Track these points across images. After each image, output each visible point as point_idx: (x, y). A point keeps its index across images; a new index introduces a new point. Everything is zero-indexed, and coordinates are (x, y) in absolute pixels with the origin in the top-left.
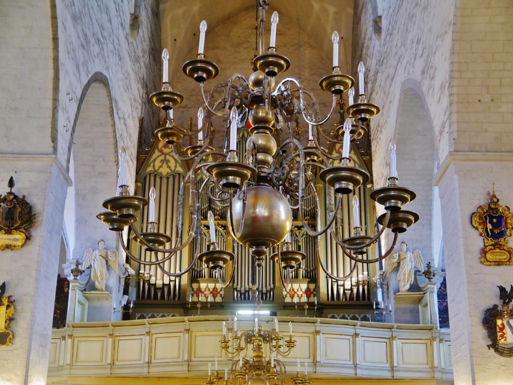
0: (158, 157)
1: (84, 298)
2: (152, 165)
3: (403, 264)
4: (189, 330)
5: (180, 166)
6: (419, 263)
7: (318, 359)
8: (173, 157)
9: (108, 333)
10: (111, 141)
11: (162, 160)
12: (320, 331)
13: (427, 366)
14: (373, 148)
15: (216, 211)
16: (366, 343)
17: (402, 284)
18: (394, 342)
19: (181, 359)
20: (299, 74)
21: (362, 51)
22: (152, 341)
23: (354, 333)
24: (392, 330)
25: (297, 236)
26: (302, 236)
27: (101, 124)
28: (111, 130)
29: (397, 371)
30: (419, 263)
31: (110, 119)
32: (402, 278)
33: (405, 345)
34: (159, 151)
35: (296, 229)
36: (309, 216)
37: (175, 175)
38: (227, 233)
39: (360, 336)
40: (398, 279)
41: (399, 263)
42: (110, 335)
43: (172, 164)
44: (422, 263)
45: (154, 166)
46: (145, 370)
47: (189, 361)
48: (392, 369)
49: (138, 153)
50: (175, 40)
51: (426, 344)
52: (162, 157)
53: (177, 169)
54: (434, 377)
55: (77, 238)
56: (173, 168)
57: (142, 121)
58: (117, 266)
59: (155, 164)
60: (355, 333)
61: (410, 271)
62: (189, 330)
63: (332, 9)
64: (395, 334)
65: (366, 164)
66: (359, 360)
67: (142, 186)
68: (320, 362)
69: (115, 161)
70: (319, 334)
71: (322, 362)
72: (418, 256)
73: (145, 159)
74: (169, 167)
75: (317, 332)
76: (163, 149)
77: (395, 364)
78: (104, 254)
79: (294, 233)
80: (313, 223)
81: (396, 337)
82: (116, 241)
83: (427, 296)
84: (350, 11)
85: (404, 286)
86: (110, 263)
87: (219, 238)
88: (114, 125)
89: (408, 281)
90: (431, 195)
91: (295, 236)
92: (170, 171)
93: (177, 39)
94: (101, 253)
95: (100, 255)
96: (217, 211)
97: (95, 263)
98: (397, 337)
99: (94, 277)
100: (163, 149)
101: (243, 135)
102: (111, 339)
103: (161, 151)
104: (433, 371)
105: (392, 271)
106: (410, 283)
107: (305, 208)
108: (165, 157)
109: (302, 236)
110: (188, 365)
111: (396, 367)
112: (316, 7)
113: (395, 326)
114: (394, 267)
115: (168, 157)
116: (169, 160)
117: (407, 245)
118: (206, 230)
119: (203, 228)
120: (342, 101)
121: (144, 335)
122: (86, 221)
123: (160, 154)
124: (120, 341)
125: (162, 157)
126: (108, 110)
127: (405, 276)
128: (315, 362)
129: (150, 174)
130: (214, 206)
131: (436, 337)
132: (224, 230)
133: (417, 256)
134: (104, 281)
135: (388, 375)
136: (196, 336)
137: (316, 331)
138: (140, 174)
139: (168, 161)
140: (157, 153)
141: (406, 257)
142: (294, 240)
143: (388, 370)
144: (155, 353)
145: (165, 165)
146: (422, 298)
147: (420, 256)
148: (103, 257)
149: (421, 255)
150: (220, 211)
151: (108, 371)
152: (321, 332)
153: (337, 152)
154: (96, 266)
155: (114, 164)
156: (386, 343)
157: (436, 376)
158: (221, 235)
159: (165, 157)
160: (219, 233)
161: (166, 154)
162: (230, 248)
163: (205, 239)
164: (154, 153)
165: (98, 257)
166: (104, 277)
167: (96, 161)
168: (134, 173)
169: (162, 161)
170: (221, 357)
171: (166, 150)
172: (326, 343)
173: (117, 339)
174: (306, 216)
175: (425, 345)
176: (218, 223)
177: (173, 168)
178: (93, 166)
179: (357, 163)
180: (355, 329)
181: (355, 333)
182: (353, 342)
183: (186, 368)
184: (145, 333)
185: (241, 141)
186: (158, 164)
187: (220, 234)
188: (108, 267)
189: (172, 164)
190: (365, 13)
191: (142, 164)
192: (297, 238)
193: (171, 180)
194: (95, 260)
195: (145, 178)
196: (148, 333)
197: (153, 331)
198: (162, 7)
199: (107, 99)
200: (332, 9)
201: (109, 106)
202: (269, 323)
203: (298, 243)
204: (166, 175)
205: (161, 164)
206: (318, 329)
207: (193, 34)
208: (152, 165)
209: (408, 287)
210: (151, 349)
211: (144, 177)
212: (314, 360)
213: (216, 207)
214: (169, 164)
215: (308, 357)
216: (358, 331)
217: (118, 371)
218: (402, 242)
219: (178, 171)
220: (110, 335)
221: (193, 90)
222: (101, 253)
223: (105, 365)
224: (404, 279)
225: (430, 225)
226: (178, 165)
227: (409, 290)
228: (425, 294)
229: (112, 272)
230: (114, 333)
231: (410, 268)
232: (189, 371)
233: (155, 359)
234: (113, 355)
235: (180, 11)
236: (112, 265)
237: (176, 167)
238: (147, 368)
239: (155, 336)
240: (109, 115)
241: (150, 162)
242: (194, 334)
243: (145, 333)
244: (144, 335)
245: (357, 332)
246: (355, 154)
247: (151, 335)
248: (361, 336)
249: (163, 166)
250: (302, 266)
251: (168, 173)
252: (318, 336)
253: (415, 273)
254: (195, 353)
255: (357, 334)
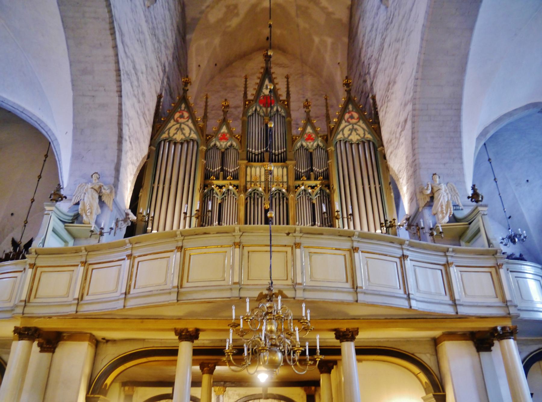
0: (173, 125)
1: (66, 232)
2: (167, 132)
3: (439, 195)
4: (182, 247)
5: (195, 133)
6: (455, 197)
7: (359, 284)
8: (188, 126)
9: (80, 261)
10: (112, 66)
11: (177, 128)
12: (358, 248)
13: (496, 300)
14: (381, 115)
15: (228, 173)
16: (418, 269)
17: (440, 216)
18: (451, 269)
19: (169, 286)
20: (303, 95)
21: (360, 56)
22: (133, 266)
23: (401, 254)
24: (448, 254)
25: (310, 195)
26: (316, 195)
27: (101, 44)
28: (111, 52)
29: (460, 305)
30: (455, 197)
31: (110, 38)
32: (440, 210)
33: (464, 274)
34: (174, 121)
35: (310, 188)
36: (322, 176)
37: (189, 140)
38: (239, 192)
39: (408, 259)
40: (435, 212)
41: (432, 198)
42: (82, 263)
43: (187, 131)
44: (458, 198)
45: (169, 134)
46: (120, 304)
47: (179, 287)
48: (454, 304)
49: (154, 122)
50: (199, 66)
51: (491, 272)
52: (178, 126)
53: (191, 136)
54: (509, 314)
55: (71, 175)
56: (187, 135)
57: (160, 97)
58: (112, 200)
59: (170, 131)
60: (403, 255)
61: (448, 202)
62: (182, 247)
63: (329, 41)
64: (450, 260)
65: (376, 131)
66: (412, 290)
67: (156, 149)
68: (361, 288)
69: (117, 91)
70: (357, 252)
71: (364, 288)
72: (453, 190)
73: (160, 127)
74: (184, 134)
75: (355, 249)
76: (178, 119)
77: (457, 297)
78: (97, 187)
79: (307, 192)
80: (326, 182)
81: (452, 263)
82: (115, 177)
83: (479, 221)
84: (346, 40)
85: (443, 218)
86: (104, 199)
87: (231, 197)
88: (115, 47)
89: (446, 214)
90: (460, 126)
91: (308, 195)
92: (184, 137)
93: (201, 65)
94: (94, 185)
95: (92, 188)
96: (230, 173)
97: (86, 195)
98: (454, 264)
99: (82, 211)
100: (178, 119)
101: (256, 110)
102: (83, 268)
103: (177, 122)
104: (507, 306)
105: (425, 206)
106: (449, 216)
107: (318, 170)
108: (180, 126)
109: (316, 195)
110: (178, 293)
111: (459, 300)
112: (316, 39)
113: (451, 250)
114: (426, 202)
115: (183, 126)
116: (183, 129)
117: (439, 177)
118: (218, 189)
119: (215, 188)
120: (347, 81)
121: (124, 259)
122: (83, 157)
123: (175, 123)
124: (94, 271)
125: (178, 126)
126: (107, 26)
127: (442, 208)
128: (355, 288)
129: (165, 140)
130: (227, 169)
131: (502, 264)
132: (236, 189)
133: (451, 190)
134: (94, 217)
135: (450, 311)
136: (190, 256)
137: (353, 247)
138: (155, 140)
139: (182, 129)
140: (172, 122)
141: (440, 188)
142: (308, 199)
143: (449, 305)
144: (135, 281)
145: (179, 132)
146: (468, 228)
147: (454, 190)
148: (95, 190)
149: (455, 189)
150: (233, 173)
151: (72, 309)
152: (360, 249)
153: (346, 122)
154: (86, 199)
155: (116, 94)
156: (441, 270)
157: (511, 312)
158: (234, 194)
159: (180, 126)
160: (231, 193)
161: (181, 124)
162: (242, 205)
163: (217, 198)
164: (170, 122)
165: (90, 190)
166: (94, 212)
167: (96, 91)
168: (149, 138)
169: (177, 129)
170: (224, 280)
171: (182, 120)
172: (367, 264)
173: (91, 267)
174: (319, 176)
175: (489, 274)
176: (230, 183)
177: (187, 135)
178: (93, 96)
179: (366, 131)
180: (402, 249)
181: (403, 255)
182: (402, 267)
183: (174, 297)
184: (125, 257)
185: (254, 115)
186: (172, 131)
187: (232, 193)
188: (101, 203)
189: (187, 131)
190: (363, 20)
191: (157, 131)
192: (310, 197)
193: (185, 145)
194: (87, 193)
195: (160, 143)
196: (130, 256)
197: (136, 253)
198: (188, 37)
199: (106, 10)
200: (329, 41)
201: (108, 20)
202: (290, 235)
203: (311, 202)
204: (180, 141)
205: (175, 131)
206: (356, 245)
207: (215, 64)
208: (167, 132)
209: (447, 219)
210: (131, 276)
211: (158, 142)
212: (353, 285)
213: (229, 170)
214: (184, 132)
215: (345, 280)
216: (406, 253)
217: (85, 309)
218: (434, 174)
219: (192, 137)
220: (82, 263)
221: (214, 106)
222: (94, 185)
223: (71, 301)
224: (442, 212)
225: (461, 158)
226: (192, 132)
227: (449, 222)
228: (470, 224)
229: (106, 209)
230: (87, 260)
231: (446, 200)
232: (178, 301)
233: (134, 288)
234: (83, 288)
235: (203, 42)
236: (106, 201)
237: (190, 134)
238: (123, 300)
239: (137, 260)
240: (108, 32)
241: (165, 130)
242: (188, 253)
243: (125, 257)
244: (124, 259)
245: (405, 254)
246: (363, 123)
247: (132, 259)
248: (411, 260)
249: (178, 133)
250: (317, 223)
251: (182, 139)
252: (356, 254)
253: (454, 206)
254: (188, 277)
255: (406, 256)
